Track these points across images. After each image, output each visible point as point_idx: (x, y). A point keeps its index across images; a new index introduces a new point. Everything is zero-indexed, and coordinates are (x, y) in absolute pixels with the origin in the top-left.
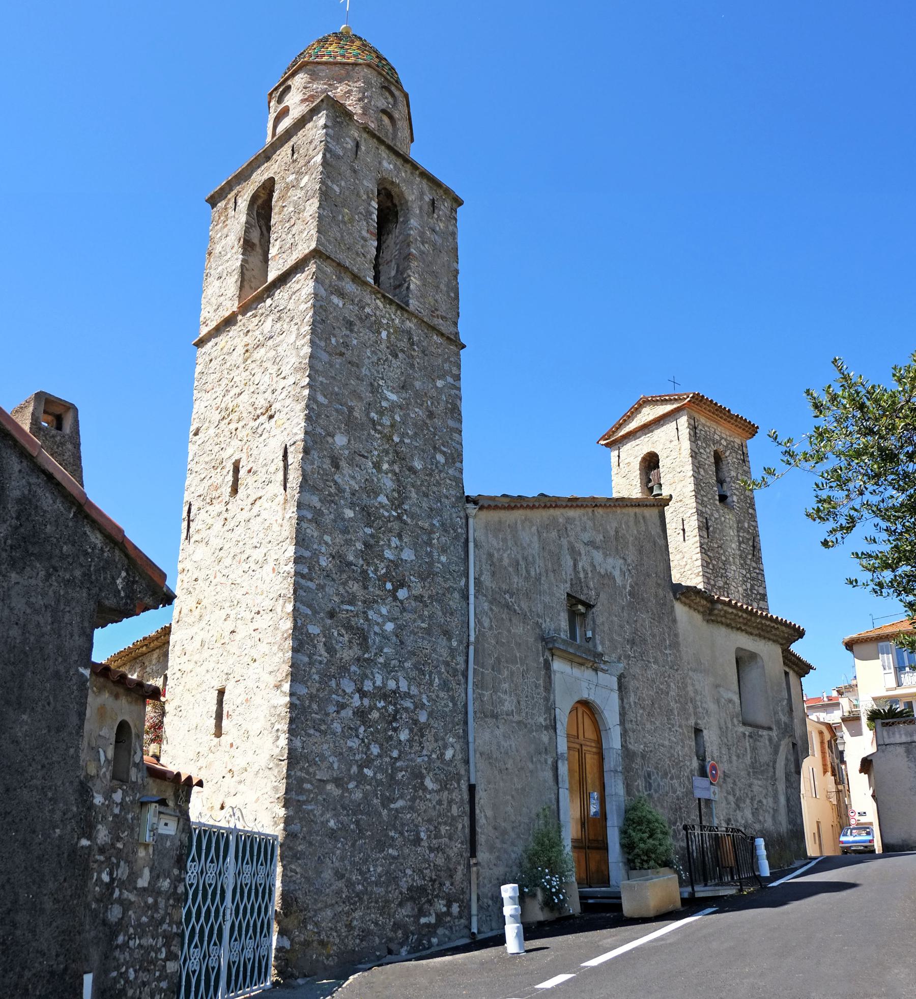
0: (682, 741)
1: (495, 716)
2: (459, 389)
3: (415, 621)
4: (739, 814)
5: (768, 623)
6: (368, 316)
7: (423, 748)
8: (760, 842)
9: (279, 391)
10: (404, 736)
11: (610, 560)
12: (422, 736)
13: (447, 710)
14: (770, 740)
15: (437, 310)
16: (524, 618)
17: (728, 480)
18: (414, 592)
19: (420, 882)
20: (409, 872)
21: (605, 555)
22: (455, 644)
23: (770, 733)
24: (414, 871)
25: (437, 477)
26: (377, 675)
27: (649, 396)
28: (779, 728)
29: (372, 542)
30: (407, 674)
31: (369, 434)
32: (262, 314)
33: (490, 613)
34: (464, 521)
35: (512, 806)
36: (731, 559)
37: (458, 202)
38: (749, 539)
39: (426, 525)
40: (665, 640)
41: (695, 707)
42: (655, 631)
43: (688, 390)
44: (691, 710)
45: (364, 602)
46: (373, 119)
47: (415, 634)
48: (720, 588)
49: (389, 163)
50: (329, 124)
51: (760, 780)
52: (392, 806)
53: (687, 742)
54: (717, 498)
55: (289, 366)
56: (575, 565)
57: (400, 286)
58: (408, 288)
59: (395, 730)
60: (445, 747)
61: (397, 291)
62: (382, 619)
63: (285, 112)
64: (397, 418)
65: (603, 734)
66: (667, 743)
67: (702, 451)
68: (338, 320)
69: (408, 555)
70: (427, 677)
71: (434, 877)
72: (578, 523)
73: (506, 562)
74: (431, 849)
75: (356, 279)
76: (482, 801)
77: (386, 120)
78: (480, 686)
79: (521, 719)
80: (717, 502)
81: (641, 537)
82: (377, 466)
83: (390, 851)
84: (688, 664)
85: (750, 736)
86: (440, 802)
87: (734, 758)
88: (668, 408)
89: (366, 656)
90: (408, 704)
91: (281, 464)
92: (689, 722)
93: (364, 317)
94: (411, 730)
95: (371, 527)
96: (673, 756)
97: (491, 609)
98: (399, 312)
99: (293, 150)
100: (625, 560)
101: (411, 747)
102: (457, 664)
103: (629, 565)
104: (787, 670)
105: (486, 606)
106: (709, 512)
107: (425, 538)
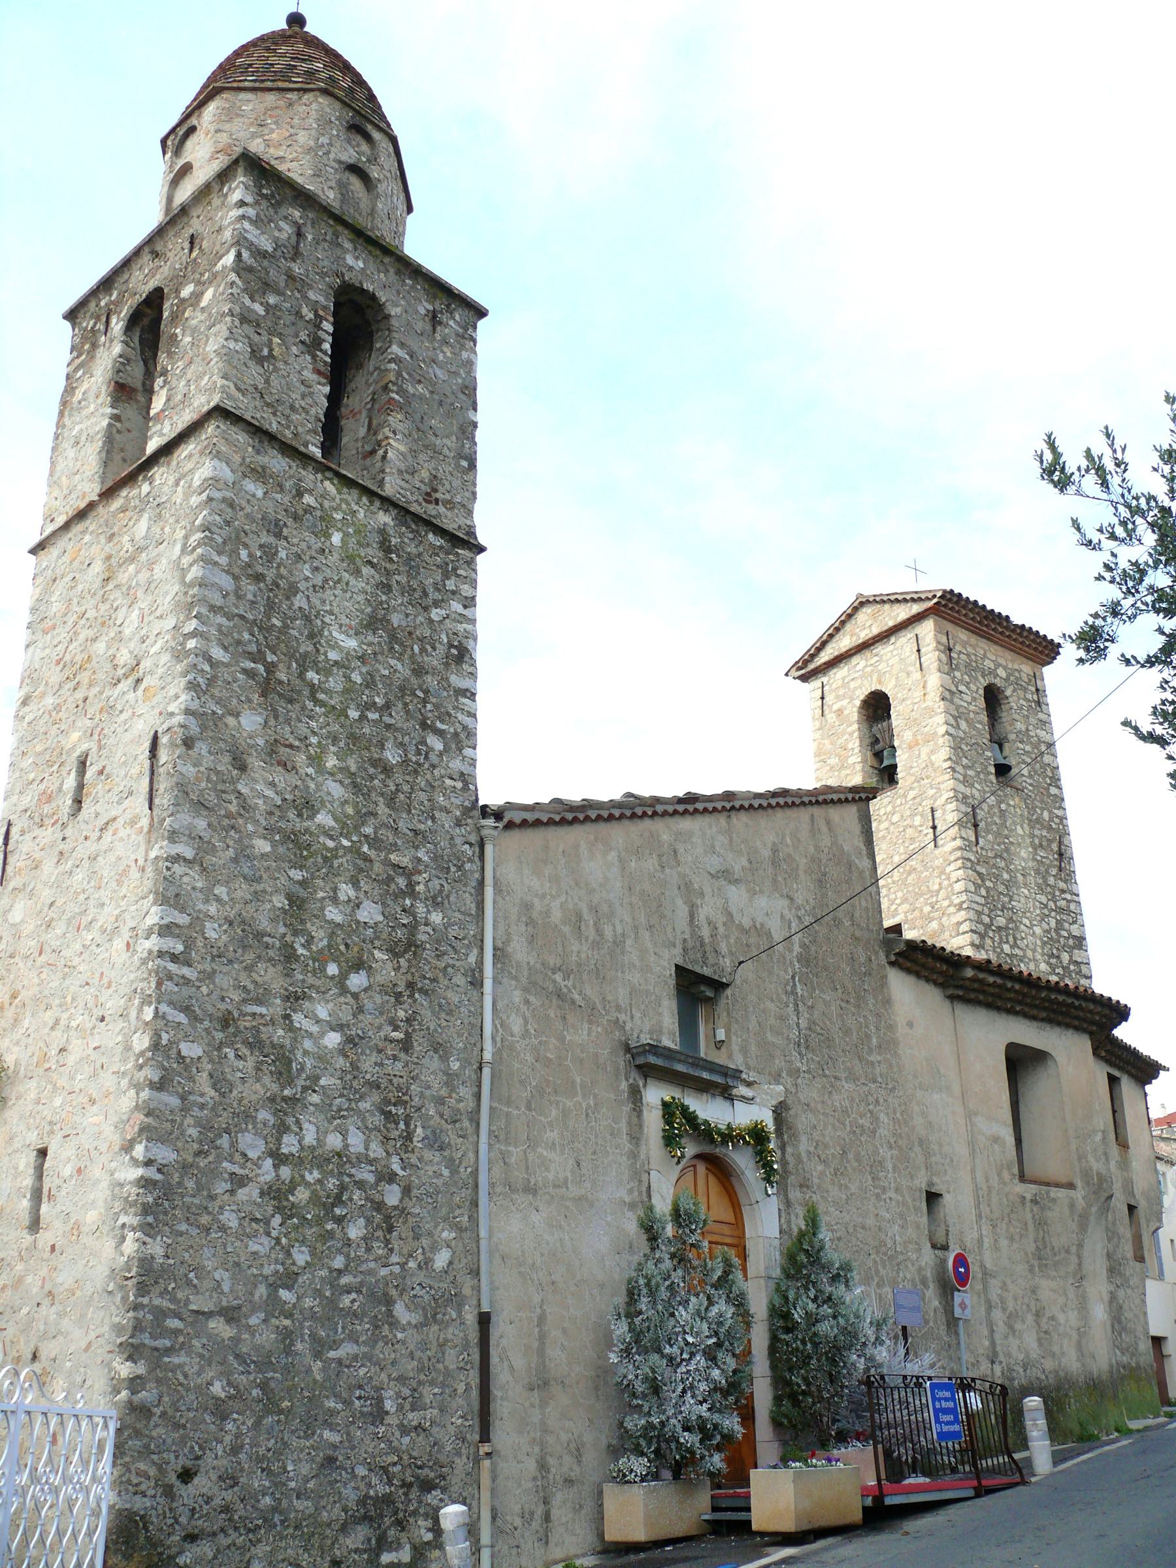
0: (901, 1215)
1: (531, 1190)
2: (473, 621)
3: (380, 1028)
4: (1014, 1343)
5: (1061, 998)
6: (309, 510)
7: (391, 1250)
8: (1033, 1402)
9: (152, 638)
10: (355, 1231)
11: (762, 902)
12: (390, 1229)
13: (439, 1182)
14: (1072, 1206)
15: (436, 491)
16: (591, 1013)
17: (1012, 737)
18: (378, 978)
19: (382, 1489)
20: (361, 1471)
21: (753, 893)
22: (455, 1066)
23: (1072, 1193)
24: (370, 1470)
25: (428, 776)
26: (306, 1126)
27: (869, 591)
28: (1088, 1183)
29: (302, 893)
30: (364, 1120)
31: (304, 708)
32: (135, 507)
33: (524, 1008)
34: (477, 850)
35: (563, 1348)
36: (1020, 878)
37: (481, 313)
38: (1050, 841)
39: (405, 861)
40: (868, 1037)
41: (928, 1154)
42: (850, 1022)
43: (936, 582)
44: (920, 1159)
45: (287, 998)
46: (333, 184)
47: (380, 1051)
48: (1000, 928)
49: (357, 258)
50: (249, 199)
51: (1053, 1278)
52: (332, 1354)
53: (911, 1218)
54: (993, 770)
55: (169, 598)
56: (692, 916)
57: (373, 452)
58: (384, 457)
59: (339, 1220)
60: (434, 1248)
61: (368, 462)
62: (319, 1028)
63: (187, 169)
64: (357, 678)
65: (746, 1211)
66: (870, 1221)
67: (962, 688)
68: (253, 520)
69: (370, 913)
70: (402, 1126)
71: (409, 1479)
72: (699, 841)
73: (556, 916)
74: (404, 1430)
75: (289, 450)
76: (504, 1342)
77: (356, 184)
78: (502, 1137)
79: (583, 1192)
80: (993, 778)
81: (824, 857)
82: (316, 761)
83: (327, 1434)
84: (915, 1076)
85: (1034, 1201)
86: (424, 1345)
87: (1004, 1243)
88: (916, 608)
89: (286, 1092)
90: (366, 1174)
91: (147, 763)
92: (917, 1182)
93: (300, 512)
94: (369, 1221)
95: (301, 868)
96: (883, 1243)
97: (527, 1002)
98: (364, 499)
99: (192, 243)
100: (791, 899)
101: (369, 1249)
102: (460, 1101)
103: (798, 908)
104: (1116, 1073)
105: (517, 996)
106: (977, 794)
107: (402, 882)
